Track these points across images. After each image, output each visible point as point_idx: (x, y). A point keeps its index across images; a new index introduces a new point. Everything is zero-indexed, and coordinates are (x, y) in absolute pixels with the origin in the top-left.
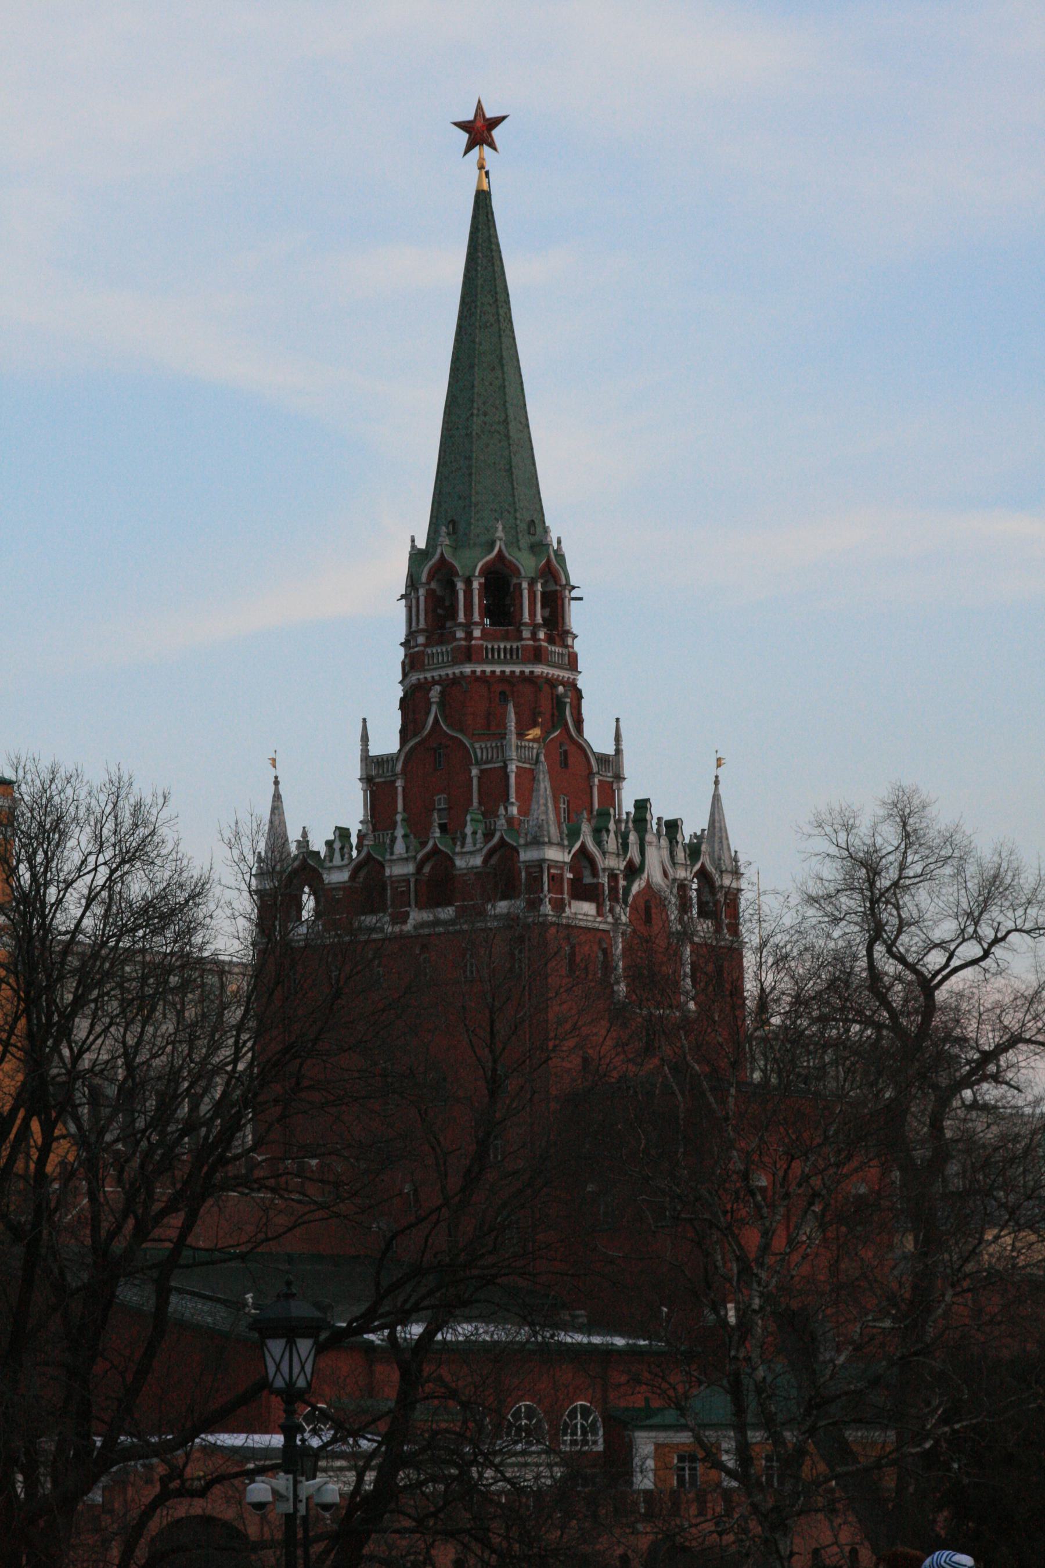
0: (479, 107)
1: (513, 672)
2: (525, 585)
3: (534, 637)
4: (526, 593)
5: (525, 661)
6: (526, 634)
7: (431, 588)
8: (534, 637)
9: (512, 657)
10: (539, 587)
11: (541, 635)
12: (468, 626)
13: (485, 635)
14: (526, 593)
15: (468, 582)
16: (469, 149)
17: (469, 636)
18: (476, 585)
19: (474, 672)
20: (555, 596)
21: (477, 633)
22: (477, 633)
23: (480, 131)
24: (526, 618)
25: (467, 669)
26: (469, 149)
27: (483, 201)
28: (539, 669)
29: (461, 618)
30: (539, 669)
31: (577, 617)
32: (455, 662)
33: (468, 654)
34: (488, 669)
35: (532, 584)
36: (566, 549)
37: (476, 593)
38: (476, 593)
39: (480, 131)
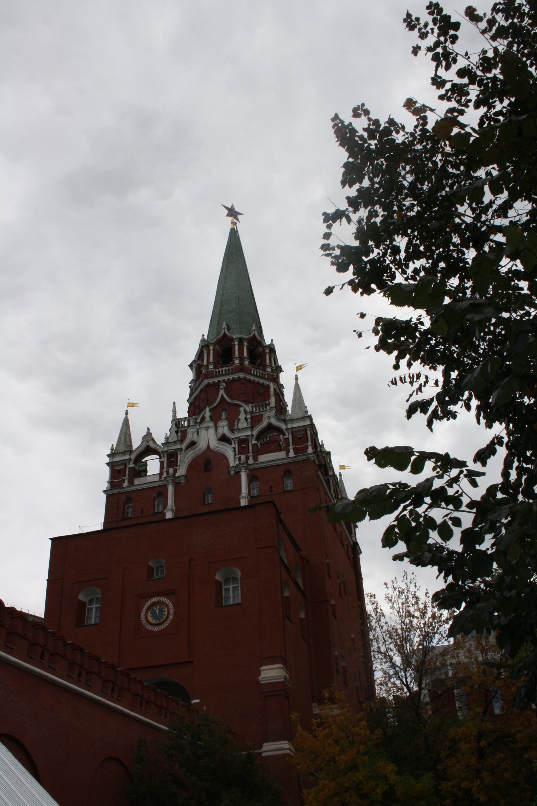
1: (229, 379)
2: (236, 343)
4: (237, 347)
5: (234, 373)
6: (237, 362)
9: (228, 373)
11: (247, 363)
12: (207, 366)
13: (215, 368)
14: (237, 347)
18: (211, 348)
21: (211, 367)
22: (211, 367)
24: (237, 354)
25: (206, 382)
28: (242, 375)
30: (242, 375)
34: (216, 380)
35: (241, 340)
36: (274, 343)
37: (211, 351)
38: (211, 351)
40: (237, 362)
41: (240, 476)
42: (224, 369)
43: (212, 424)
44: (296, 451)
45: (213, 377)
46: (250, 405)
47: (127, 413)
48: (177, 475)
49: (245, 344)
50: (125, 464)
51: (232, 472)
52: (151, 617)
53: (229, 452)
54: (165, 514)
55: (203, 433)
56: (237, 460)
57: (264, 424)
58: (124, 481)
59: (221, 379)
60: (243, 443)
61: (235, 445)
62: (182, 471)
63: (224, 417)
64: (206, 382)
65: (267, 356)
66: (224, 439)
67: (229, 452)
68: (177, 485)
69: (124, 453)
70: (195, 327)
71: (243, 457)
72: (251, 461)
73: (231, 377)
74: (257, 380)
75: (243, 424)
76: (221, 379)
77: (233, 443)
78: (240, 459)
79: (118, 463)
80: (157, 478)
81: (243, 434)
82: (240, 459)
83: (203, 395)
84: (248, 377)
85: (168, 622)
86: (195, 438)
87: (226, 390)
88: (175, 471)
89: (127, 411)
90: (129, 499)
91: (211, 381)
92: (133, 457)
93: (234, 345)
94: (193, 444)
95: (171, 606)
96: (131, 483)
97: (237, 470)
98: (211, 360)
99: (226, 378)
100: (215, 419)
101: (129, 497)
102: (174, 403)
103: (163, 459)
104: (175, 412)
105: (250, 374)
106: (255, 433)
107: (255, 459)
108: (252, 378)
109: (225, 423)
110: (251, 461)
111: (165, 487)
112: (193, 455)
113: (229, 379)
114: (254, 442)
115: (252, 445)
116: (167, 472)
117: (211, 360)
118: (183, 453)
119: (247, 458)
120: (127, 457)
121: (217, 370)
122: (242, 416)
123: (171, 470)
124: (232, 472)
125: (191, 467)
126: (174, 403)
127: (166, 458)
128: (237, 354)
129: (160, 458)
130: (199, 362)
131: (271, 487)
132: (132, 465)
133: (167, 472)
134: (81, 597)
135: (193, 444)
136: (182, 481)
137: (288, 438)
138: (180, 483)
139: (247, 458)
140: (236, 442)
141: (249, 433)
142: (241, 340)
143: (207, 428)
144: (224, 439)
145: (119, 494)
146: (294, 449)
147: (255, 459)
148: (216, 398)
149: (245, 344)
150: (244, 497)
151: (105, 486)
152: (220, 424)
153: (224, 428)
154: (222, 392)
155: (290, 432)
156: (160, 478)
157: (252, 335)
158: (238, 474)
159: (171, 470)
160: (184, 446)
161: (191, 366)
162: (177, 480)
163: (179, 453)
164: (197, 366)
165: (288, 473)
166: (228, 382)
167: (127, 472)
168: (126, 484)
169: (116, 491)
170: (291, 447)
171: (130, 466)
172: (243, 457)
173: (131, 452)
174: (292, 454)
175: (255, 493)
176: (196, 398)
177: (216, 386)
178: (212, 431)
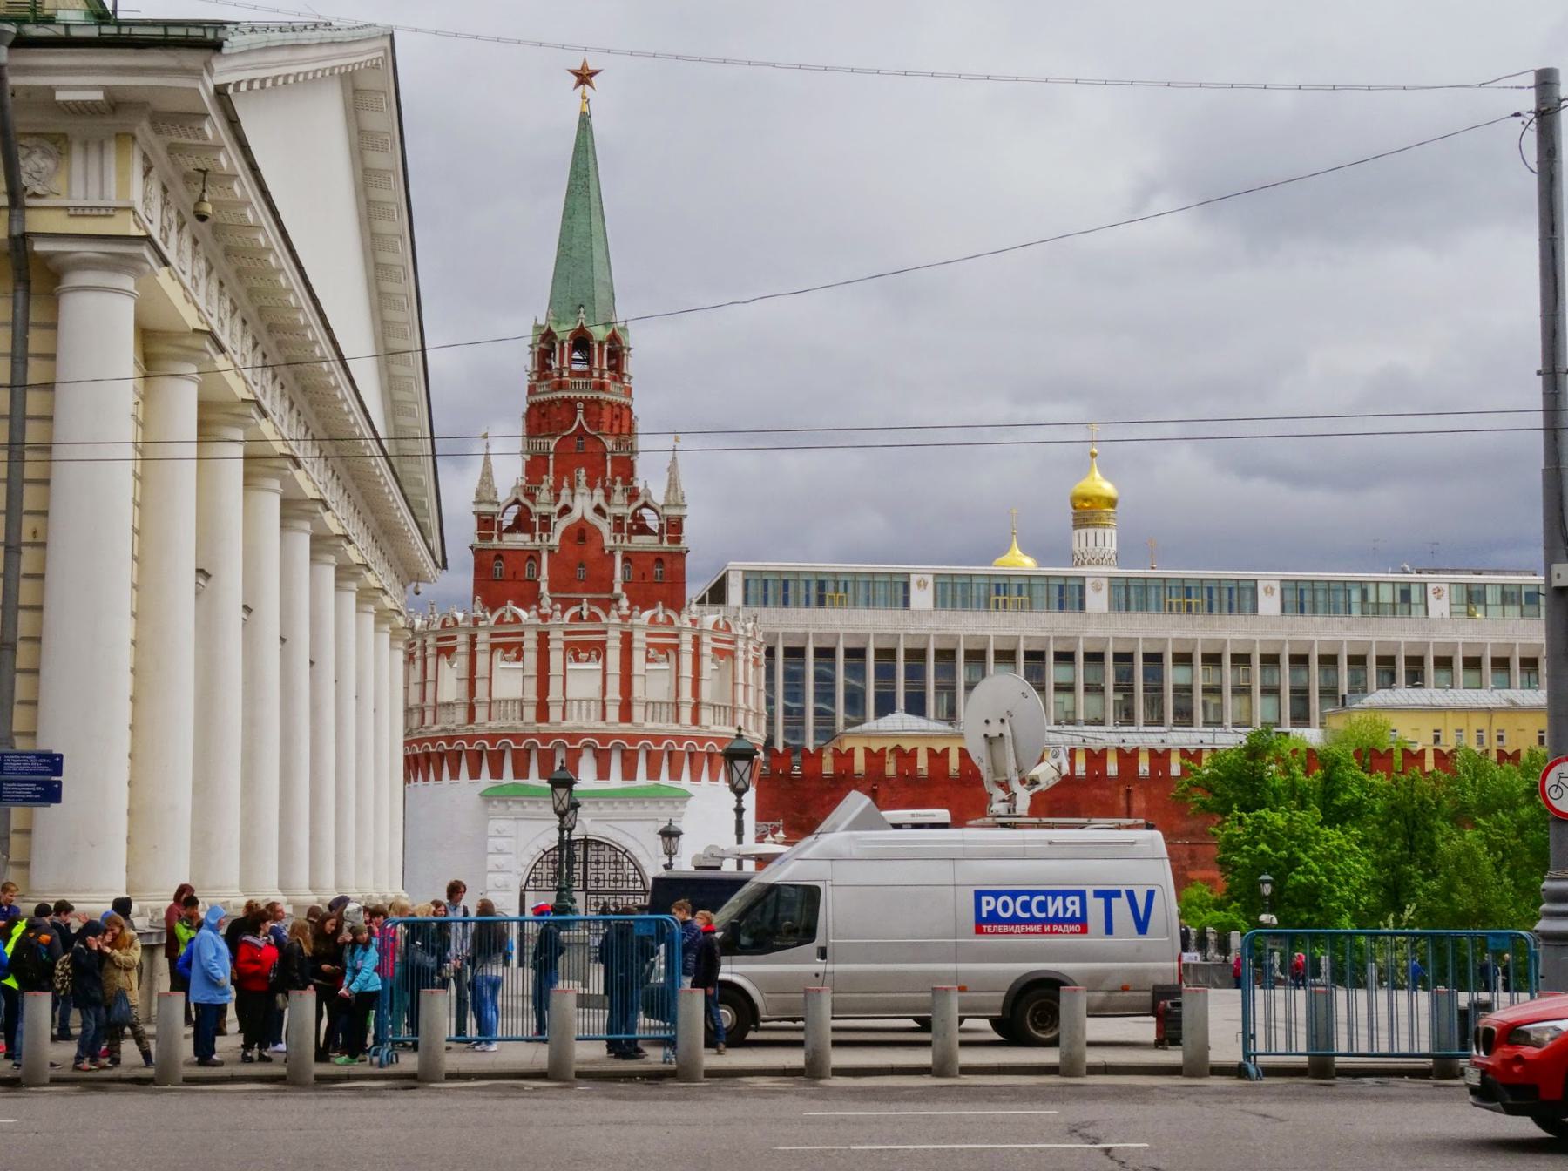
0: (585, 63)
3: (601, 376)
6: (596, 374)
7: (546, 345)
8: (601, 376)
15: (562, 344)
16: (577, 86)
17: (561, 375)
20: (616, 353)
21: (566, 374)
23: (584, 77)
25: (559, 395)
26: (577, 86)
27: (585, 120)
28: (602, 396)
30: (602, 396)
31: (631, 366)
32: (555, 390)
33: (561, 386)
39: (584, 77)
40: (596, 374)
43: (587, 491)
44: (670, 540)
45: (567, 389)
53: (605, 527)
55: (578, 498)
57: (640, 502)
60: (618, 520)
62: (555, 540)
63: (599, 483)
64: (559, 395)
66: (598, 510)
67: (605, 527)
68: (551, 552)
69: (492, 503)
72: (625, 543)
75: (619, 497)
79: (485, 514)
81: (618, 511)
83: (553, 408)
84: (609, 397)
91: (566, 394)
96: (500, 538)
100: (591, 485)
101: (499, 555)
106: (630, 511)
110: (625, 543)
125: (565, 535)
135: (566, 510)
142: (601, 344)
154: (580, 417)
156: (533, 540)
158: (612, 553)
160: (556, 510)
166: (585, 401)
168: (495, 541)
169: (486, 545)
174: (665, 544)
176: (541, 404)
177: (570, 403)
178: (587, 499)
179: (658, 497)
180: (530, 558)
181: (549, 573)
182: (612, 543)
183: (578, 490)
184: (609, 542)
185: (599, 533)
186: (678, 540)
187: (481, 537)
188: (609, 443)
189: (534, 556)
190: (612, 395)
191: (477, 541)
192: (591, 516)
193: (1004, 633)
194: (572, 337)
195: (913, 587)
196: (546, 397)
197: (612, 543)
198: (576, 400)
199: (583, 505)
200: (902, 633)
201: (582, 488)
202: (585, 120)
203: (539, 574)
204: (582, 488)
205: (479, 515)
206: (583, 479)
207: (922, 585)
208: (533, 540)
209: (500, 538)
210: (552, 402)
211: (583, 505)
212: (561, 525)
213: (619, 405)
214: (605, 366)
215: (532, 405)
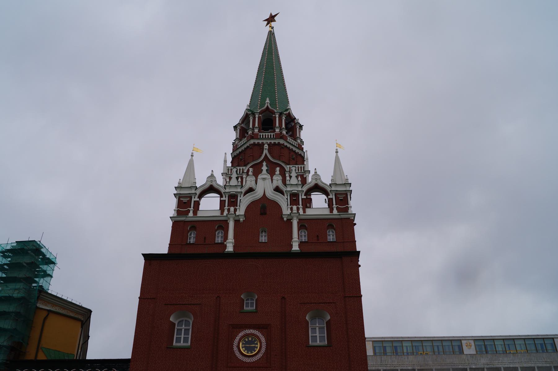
0: (271, 14)
1: (271, 143)
2: (277, 116)
4: (277, 119)
5: (275, 139)
6: (277, 130)
8: (281, 133)
10: (284, 118)
11: (284, 132)
12: (253, 129)
14: (277, 119)
15: (253, 114)
18: (257, 116)
19: (254, 143)
22: (256, 131)
24: (277, 125)
25: (252, 142)
28: (282, 141)
29: (251, 126)
30: (282, 141)
33: (252, 137)
34: (260, 142)
35: (281, 114)
37: (257, 119)
38: (257, 119)
39: (271, 19)
41: (291, 223)
42: (267, 134)
43: (268, 176)
45: (258, 139)
46: (288, 166)
47: (192, 156)
48: (237, 213)
49: (284, 118)
50: (191, 198)
51: (285, 219)
52: (243, 347)
53: (283, 202)
54: (225, 247)
56: (289, 209)
57: (312, 184)
58: (189, 211)
59: (265, 141)
61: (287, 197)
62: (241, 211)
64: (252, 142)
65: (298, 129)
66: (277, 189)
68: (237, 222)
70: (238, 98)
71: (295, 208)
73: (273, 142)
74: (291, 147)
76: (265, 141)
77: (286, 195)
78: (291, 209)
79: (185, 196)
80: (218, 214)
81: (295, 189)
82: (291, 209)
84: (286, 144)
85: (260, 355)
86: (253, 185)
87: (269, 150)
88: (235, 210)
89: (192, 153)
90: (193, 228)
91: (256, 141)
92: (198, 192)
93: (275, 117)
94: (251, 190)
95: (263, 340)
96: (195, 213)
97: (289, 218)
98: (257, 125)
99: (269, 142)
100: (271, 173)
102: (226, 154)
103: (223, 199)
104: (225, 161)
105: (286, 140)
107: (304, 212)
108: (288, 145)
109: (280, 178)
110: (301, 211)
111: (226, 223)
112: (251, 199)
113: (271, 143)
114: (305, 197)
115: (302, 199)
116: (229, 210)
117: (257, 125)
118: (242, 196)
119: (298, 209)
120: (193, 191)
121: (261, 134)
122: (294, 174)
123: (232, 209)
124: (285, 219)
126: (226, 154)
127: (227, 198)
128: (277, 125)
129: (221, 196)
130: (242, 125)
131: (318, 236)
132: (197, 199)
133: (229, 210)
134: (171, 319)
135: (251, 190)
136: (241, 220)
137: (332, 199)
138: (239, 220)
139: (298, 209)
140: (289, 194)
141: (300, 189)
143: (264, 179)
144: (277, 189)
145: (184, 222)
146: (337, 208)
147: (304, 212)
148: (261, 156)
149: (284, 118)
150: (296, 241)
151: (172, 213)
152: (274, 177)
153: (278, 180)
154: (266, 152)
155: (334, 194)
156: (222, 213)
157: (288, 112)
158: (289, 221)
159: (232, 209)
160: (243, 190)
161: (235, 127)
162: (237, 218)
163: (239, 195)
164: (243, 128)
165: (331, 226)
167: (192, 206)
168: (191, 214)
170: (334, 206)
171: (195, 200)
172: (295, 208)
173: (196, 188)
174: (335, 212)
175: (304, 239)
179: (326, 180)
180: (220, 227)
181: (235, 237)
182: (289, 212)
183: (260, 177)
184: (286, 211)
185: (277, 206)
186: (346, 209)
187: (179, 213)
188: (287, 168)
189: (222, 225)
190: (289, 142)
191: (176, 215)
192: (271, 195)
193: (525, 365)
194: (260, 113)
195: (465, 347)
196: (243, 148)
197: (289, 212)
198: (263, 144)
199: (264, 185)
200: (468, 367)
201: (264, 174)
202: (271, 35)
203: (226, 237)
204: (264, 174)
205: (179, 196)
206: (264, 168)
207: (469, 346)
208: (222, 213)
209: (195, 213)
210: (248, 147)
211: (264, 185)
212: (244, 202)
213: (295, 151)
214: (284, 126)
215: (233, 158)
